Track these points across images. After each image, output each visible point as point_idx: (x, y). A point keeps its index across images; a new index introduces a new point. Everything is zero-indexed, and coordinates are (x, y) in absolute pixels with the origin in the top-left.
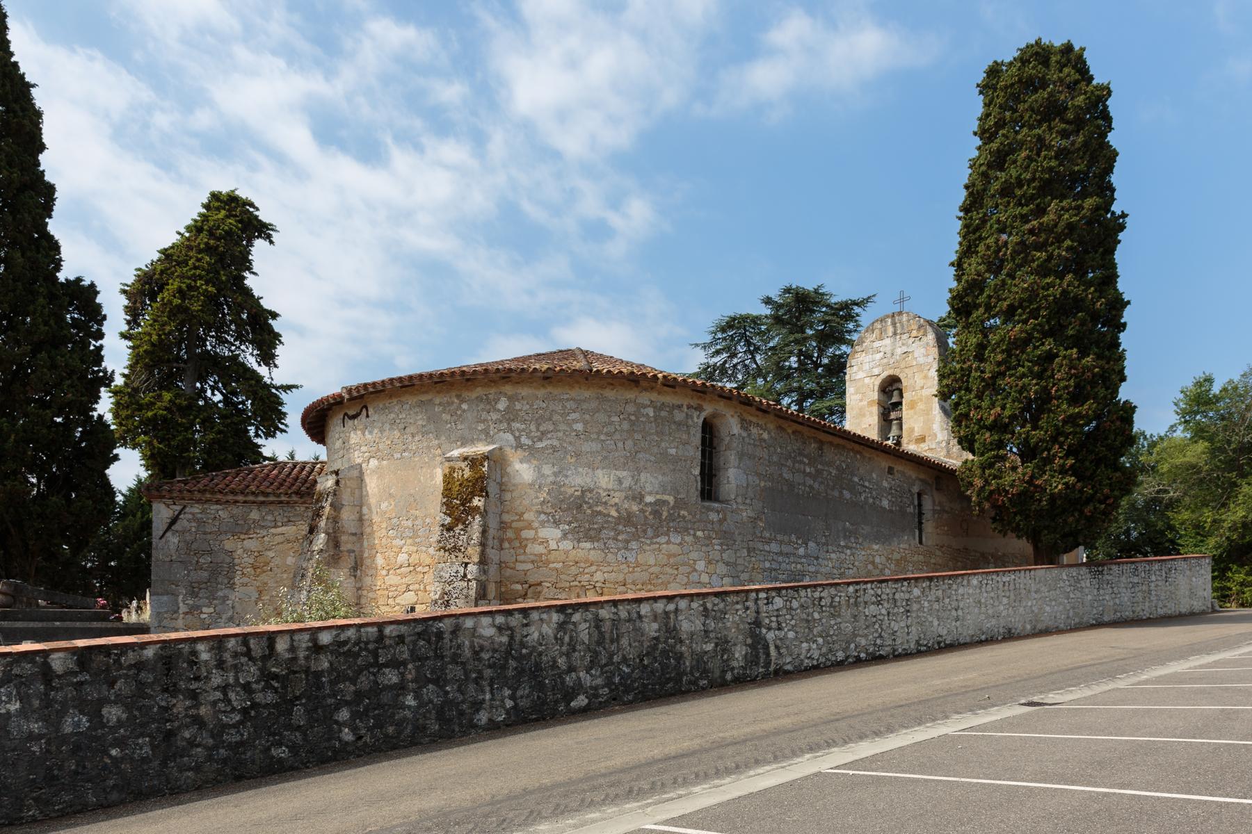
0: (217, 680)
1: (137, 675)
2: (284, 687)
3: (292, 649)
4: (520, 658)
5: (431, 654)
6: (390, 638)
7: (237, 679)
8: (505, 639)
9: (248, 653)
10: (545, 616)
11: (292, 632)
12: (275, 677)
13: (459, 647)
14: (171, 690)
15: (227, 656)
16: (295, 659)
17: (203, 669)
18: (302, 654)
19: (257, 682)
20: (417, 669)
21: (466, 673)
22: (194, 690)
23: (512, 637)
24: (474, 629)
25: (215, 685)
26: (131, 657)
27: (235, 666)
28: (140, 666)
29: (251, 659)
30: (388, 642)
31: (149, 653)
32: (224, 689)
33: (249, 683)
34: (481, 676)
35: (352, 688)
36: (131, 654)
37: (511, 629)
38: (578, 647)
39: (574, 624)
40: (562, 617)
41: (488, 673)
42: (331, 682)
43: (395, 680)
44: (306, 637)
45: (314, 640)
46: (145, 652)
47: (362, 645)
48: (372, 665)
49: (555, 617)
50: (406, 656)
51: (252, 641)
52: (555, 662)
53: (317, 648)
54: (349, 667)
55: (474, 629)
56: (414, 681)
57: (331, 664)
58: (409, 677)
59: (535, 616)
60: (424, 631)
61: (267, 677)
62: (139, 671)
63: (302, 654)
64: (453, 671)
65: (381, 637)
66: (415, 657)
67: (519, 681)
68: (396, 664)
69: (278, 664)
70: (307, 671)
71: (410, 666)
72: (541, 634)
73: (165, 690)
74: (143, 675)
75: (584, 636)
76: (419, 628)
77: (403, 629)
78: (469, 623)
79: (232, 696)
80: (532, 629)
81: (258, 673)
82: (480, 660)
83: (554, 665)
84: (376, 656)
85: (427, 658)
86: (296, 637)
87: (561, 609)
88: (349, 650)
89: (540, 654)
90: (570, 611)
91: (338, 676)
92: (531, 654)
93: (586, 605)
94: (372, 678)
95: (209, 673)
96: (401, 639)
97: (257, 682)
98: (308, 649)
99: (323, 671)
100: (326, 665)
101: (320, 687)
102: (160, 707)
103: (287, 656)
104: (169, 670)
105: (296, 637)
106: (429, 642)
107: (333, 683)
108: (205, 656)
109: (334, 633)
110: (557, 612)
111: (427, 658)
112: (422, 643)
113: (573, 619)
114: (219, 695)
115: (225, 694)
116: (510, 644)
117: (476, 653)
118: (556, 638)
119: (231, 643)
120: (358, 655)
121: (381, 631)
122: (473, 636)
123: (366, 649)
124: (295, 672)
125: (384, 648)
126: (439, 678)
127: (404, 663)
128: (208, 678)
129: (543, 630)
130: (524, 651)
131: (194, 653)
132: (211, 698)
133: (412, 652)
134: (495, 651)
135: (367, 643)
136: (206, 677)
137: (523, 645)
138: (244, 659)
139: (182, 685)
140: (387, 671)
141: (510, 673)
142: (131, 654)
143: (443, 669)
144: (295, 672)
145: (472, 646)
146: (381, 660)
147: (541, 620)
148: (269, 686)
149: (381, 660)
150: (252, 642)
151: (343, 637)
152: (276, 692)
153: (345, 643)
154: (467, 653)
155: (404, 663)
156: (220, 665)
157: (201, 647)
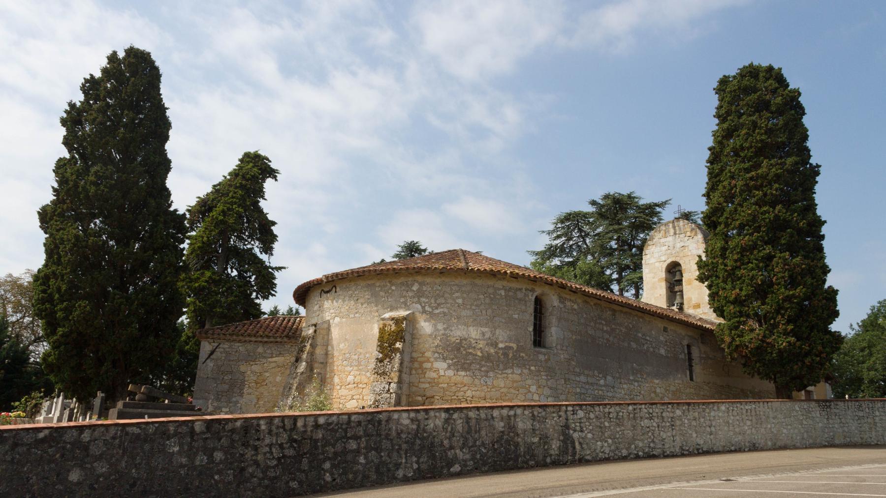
0: (267, 441)
2: (299, 447)
3: (305, 426)
4: (423, 439)
7: (277, 441)
8: (415, 427)
9: (284, 427)
10: (437, 414)
11: (305, 416)
12: (295, 441)
13: (390, 430)
14: (246, 445)
15: (274, 428)
16: (305, 431)
18: (309, 429)
19: (287, 443)
20: (367, 441)
23: (419, 426)
26: (229, 426)
27: (277, 434)
28: (233, 431)
29: (285, 430)
30: (353, 424)
31: (238, 424)
32: (270, 446)
33: (282, 444)
34: (400, 449)
35: (333, 450)
37: (418, 420)
39: (454, 420)
40: (447, 416)
41: (404, 446)
42: (322, 446)
43: (355, 447)
44: (312, 419)
45: (316, 421)
48: (343, 438)
49: (443, 415)
50: (361, 433)
52: (442, 442)
53: (317, 426)
55: (398, 419)
56: (365, 448)
58: (362, 445)
59: (432, 414)
61: (292, 440)
63: (309, 429)
64: (386, 444)
65: (349, 421)
68: (356, 438)
70: (311, 439)
73: (243, 445)
75: (459, 428)
76: (369, 418)
77: (361, 417)
78: (396, 416)
79: (274, 450)
80: (430, 421)
82: (400, 438)
83: (442, 445)
84: (346, 432)
85: (373, 435)
87: (447, 410)
89: (434, 437)
93: (461, 409)
96: (359, 423)
97: (287, 443)
98: (313, 426)
100: (321, 436)
101: (316, 448)
103: (302, 429)
105: (307, 419)
106: (374, 426)
107: (324, 446)
108: (263, 427)
111: (373, 435)
114: (267, 449)
117: (399, 434)
119: (276, 421)
120: (337, 431)
121: (349, 418)
128: (263, 439)
129: (436, 422)
131: (258, 425)
132: (264, 451)
133: (365, 431)
134: (409, 433)
135: (342, 425)
137: (424, 431)
138: (281, 430)
139: (251, 442)
140: (351, 441)
141: (417, 447)
142: (230, 424)
143: (380, 442)
145: (397, 430)
146: (349, 435)
148: (292, 446)
149: (349, 435)
151: (330, 421)
153: (331, 424)
154: (394, 433)
156: (270, 432)
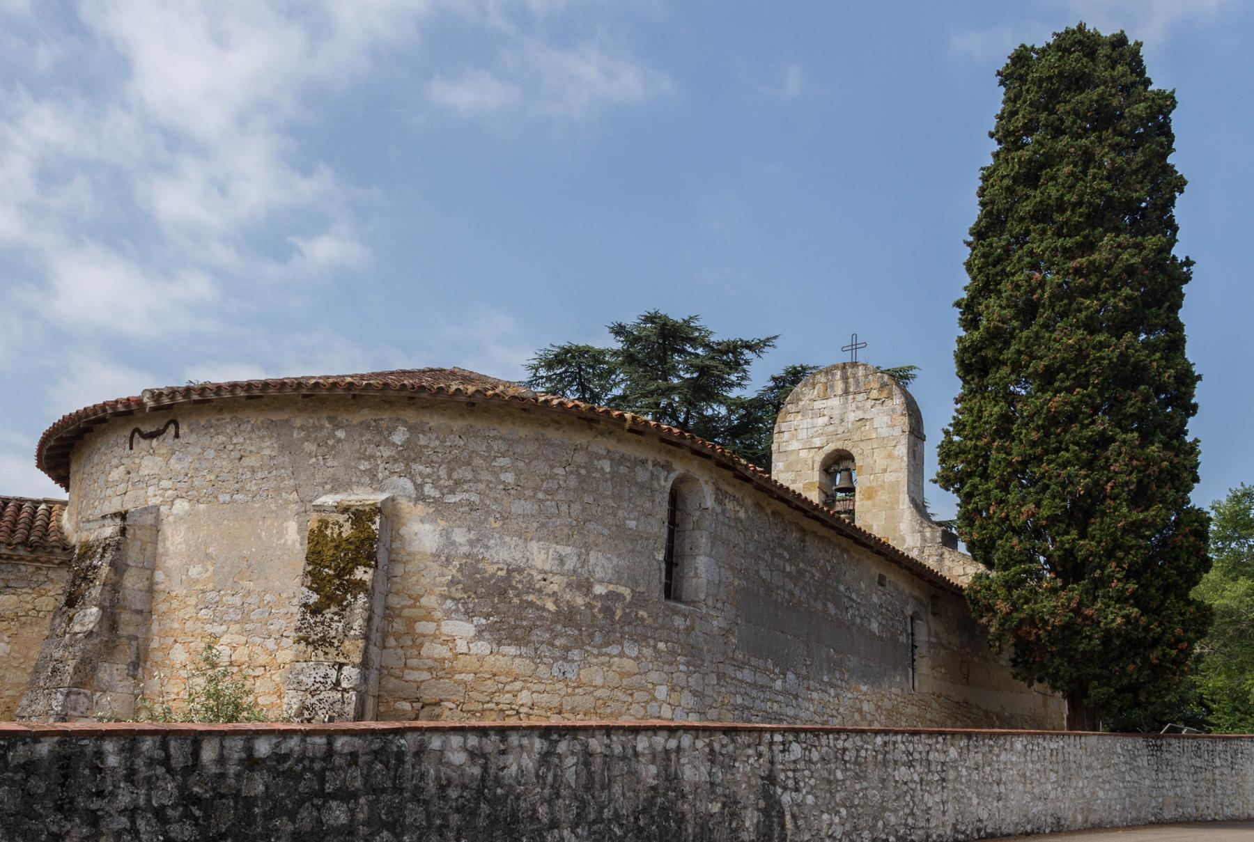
0: (124, 799)
1: (25, 780)
2: (207, 818)
3: (221, 760)
4: (494, 801)
5: (389, 784)
6: (341, 754)
7: (149, 801)
8: (477, 771)
9: (166, 762)
10: (525, 741)
11: (222, 735)
12: (197, 800)
13: (423, 776)
14: (65, 808)
15: (140, 763)
16: (222, 776)
17: (109, 781)
18: (232, 770)
19: (174, 807)
20: (371, 805)
21: (429, 817)
22: (94, 812)
23: (485, 769)
24: (442, 751)
25: (122, 806)
26: (19, 754)
27: (148, 779)
28: (30, 767)
29: (170, 770)
30: (338, 761)
31: (44, 748)
32: (132, 812)
33: (163, 807)
34: (445, 825)
35: (290, 827)
36: (21, 748)
37: (484, 756)
38: (563, 792)
39: (573, 753)
40: (546, 744)
41: (455, 819)
42: (264, 814)
43: (343, 819)
44: (239, 743)
45: (249, 750)
46: (38, 746)
47: (306, 763)
48: (316, 794)
49: (538, 744)
50: (358, 784)
51: (173, 744)
52: (535, 811)
53: (251, 762)
54: (289, 795)
55: (442, 751)
56: (367, 823)
57: (267, 788)
58: (361, 816)
59: (514, 739)
60: (383, 748)
61: (187, 799)
62: (29, 774)
63: (232, 770)
64: (413, 813)
65: (330, 752)
66: (372, 789)
67: (491, 836)
68: (346, 795)
69: (201, 783)
70: (237, 796)
71: (362, 801)
72: (520, 767)
73: (59, 808)
74: (32, 781)
75: (570, 776)
76: (376, 745)
77: (358, 742)
78: (436, 742)
79: (141, 824)
80: (510, 758)
81: (176, 792)
82: (445, 798)
83: (534, 817)
84: (322, 781)
85: (384, 790)
86: (227, 743)
87: (545, 732)
88: (290, 769)
89: (518, 798)
90: (555, 737)
91: (274, 807)
92: (507, 796)
93: (573, 731)
94: (315, 814)
95: (116, 787)
96: (354, 755)
97: (174, 807)
98: (241, 761)
99: (256, 797)
100: (261, 788)
101: (250, 820)
102: (51, 834)
103: (214, 770)
104: (66, 777)
105: (227, 743)
106: (387, 766)
107: (269, 816)
108: (112, 761)
109: (274, 741)
110: (541, 736)
111: (384, 790)
112: (379, 766)
113: (559, 750)
114: (124, 822)
115: (133, 822)
116: (483, 779)
117: (442, 788)
118: (537, 776)
119: (147, 744)
120: (299, 777)
121: (330, 744)
122: (440, 762)
123: (311, 769)
124: (222, 796)
125: (332, 769)
126: (396, 821)
127: (354, 795)
128: (113, 794)
129: (522, 761)
130: (499, 791)
131: (100, 754)
132: (115, 826)
133: (366, 778)
134: (465, 787)
135: (312, 760)
136: (112, 793)
137: (498, 782)
138: (160, 770)
139: (81, 802)
140: (334, 804)
141: (482, 822)
142: (21, 748)
143: (401, 808)
144: (222, 796)
145: (438, 778)
146: (329, 788)
147: (521, 746)
148: (187, 815)
149: (329, 788)
150: (173, 744)
151: (284, 749)
152: (197, 824)
153: (286, 757)
154: (432, 787)
155: (354, 795)
156: (131, 776)
157: (109, 746)
